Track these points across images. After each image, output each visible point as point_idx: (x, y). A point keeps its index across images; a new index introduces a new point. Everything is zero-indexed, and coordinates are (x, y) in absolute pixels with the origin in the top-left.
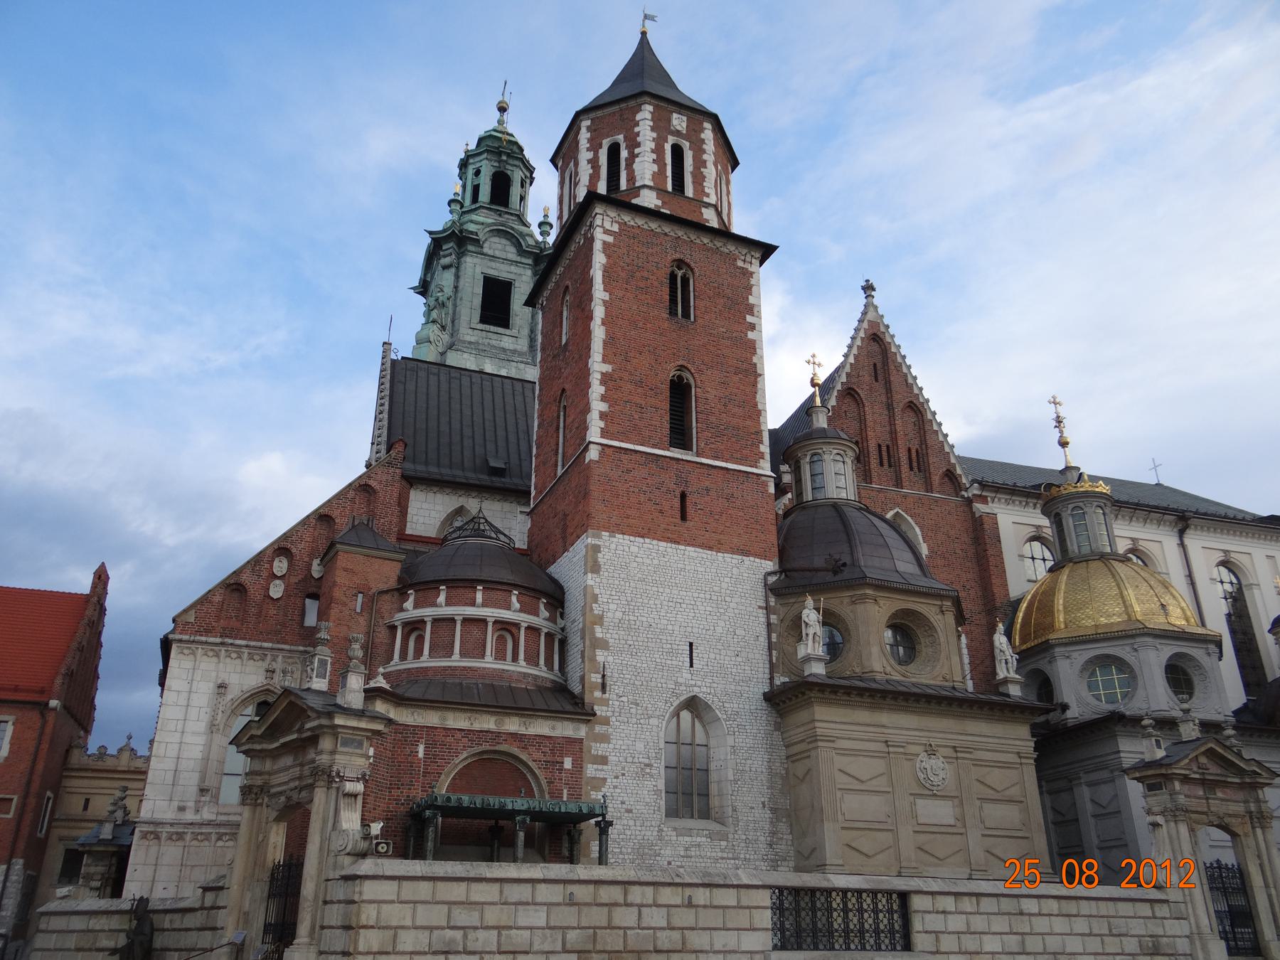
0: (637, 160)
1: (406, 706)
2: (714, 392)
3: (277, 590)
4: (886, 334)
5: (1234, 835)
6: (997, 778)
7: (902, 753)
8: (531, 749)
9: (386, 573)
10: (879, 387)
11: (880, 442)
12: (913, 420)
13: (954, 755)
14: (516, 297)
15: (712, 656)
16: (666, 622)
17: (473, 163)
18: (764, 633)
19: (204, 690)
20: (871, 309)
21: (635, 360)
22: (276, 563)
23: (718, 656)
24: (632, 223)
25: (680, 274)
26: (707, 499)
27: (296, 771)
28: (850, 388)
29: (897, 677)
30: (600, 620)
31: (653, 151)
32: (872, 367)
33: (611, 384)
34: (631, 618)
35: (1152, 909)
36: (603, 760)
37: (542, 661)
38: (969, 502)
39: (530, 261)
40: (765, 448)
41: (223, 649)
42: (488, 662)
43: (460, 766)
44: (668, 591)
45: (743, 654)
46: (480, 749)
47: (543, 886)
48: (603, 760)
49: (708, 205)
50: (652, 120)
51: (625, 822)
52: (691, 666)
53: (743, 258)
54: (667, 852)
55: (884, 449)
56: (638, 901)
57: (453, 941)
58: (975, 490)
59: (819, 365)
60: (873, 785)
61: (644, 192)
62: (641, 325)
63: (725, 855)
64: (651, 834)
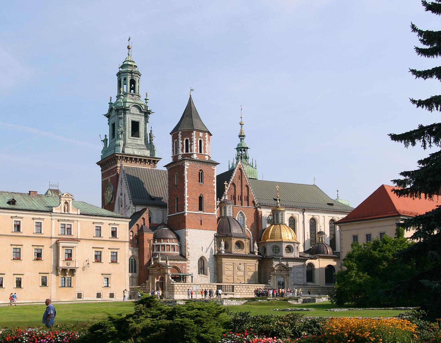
0: (192, 146)
2: (207, 198)
5: (284, 277)
10: (240, 181)
14: (140, 127)
17: (124, 75)
27: (159, 272)
32: (238, 176)
36: (189, 266)
38: (256, 209)
39: (144, 114)
40: (216, 209)
48: (189, 266)
49: (206, 155)
55: (239, 196)
57: (183, 291)
62: (194, 186)
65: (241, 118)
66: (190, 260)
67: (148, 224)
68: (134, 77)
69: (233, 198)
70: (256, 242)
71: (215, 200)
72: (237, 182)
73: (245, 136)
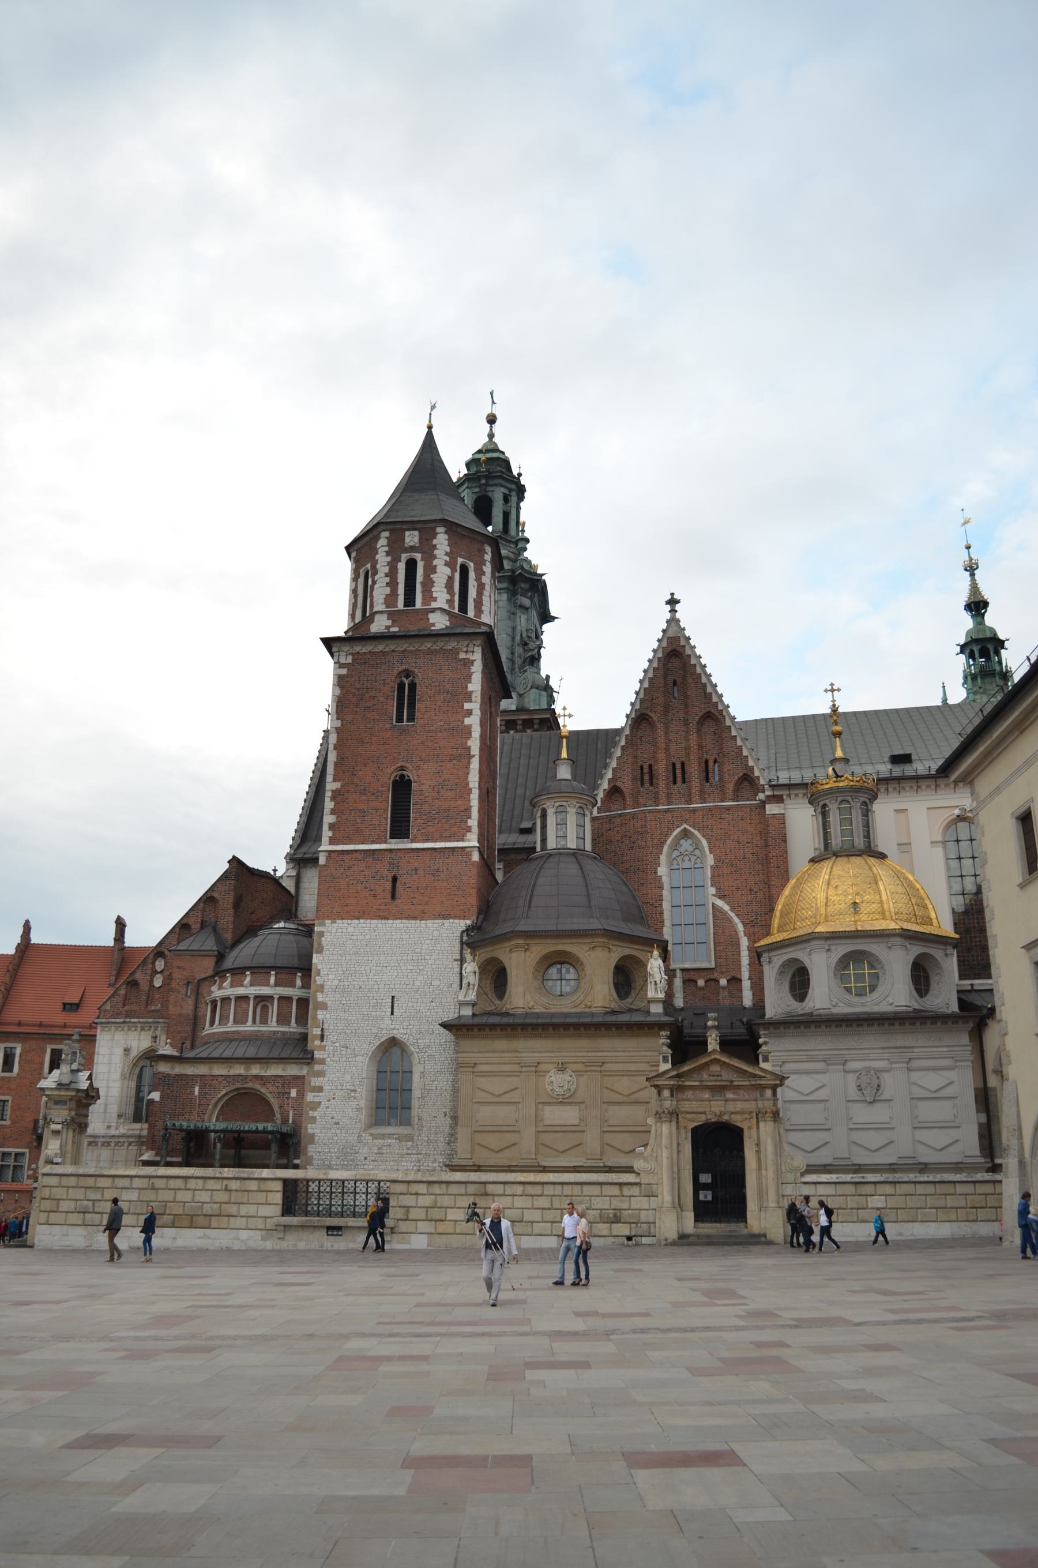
1: (187, 1063)
2: (429, 783)
3: (158, 982)
4: (687, 647)
6: (624, 1085)
7: (532, 1071)
8: (268, 1085)
9: (207, 966)
11: (674, 760)
12: (713, 730)
13: (585, 1069)
15: (410, 1004)
16: (373, 983)
18: (458, 980)
19: (119, 1051)
20: (673, 624)
21: (360, 773)
22: (157, 963)
23: (415, 1005)
24: (364, 650)
25: (407, 682)
26: (415, 877)
28: (643, 714)
29: (538, 1010)
30: (321, 988)
31: (387, 575)
33: (339, 798)
34: (346, 983)
35: (621, 1190)
36: (320, 1089)
37: (293, 1020)
38: (763, 804)
40: (473, 822)
41: (126, 1025)
42: (248, 1027)
43: (225, 1099)
44: (376, 958)
45: (437, 1000)
46: (232, 1087)
47: (137, 1179)
48: (320, 1089)
49: (433, 610)
50: (388, 545)
51: (334, 1131)
52: (392, 1013)
53: (465, 649)
54: (365, 1151)
55: (678, 766)
56: (193, 1187)
58: (768, 793)
59: (570, 716)
60: (505, 1098)
61: (377, 617)
62: (367, 740)
63: (410, 1152)
64: (353, 1139)
65: (968, 547)
66: (329, 1059)
67: (231, 919)
68: (490, 489)
69: (646, 777)
70: (656, 953)
71: (471, 785)
72: (659, 709)
73: (985, 604)
